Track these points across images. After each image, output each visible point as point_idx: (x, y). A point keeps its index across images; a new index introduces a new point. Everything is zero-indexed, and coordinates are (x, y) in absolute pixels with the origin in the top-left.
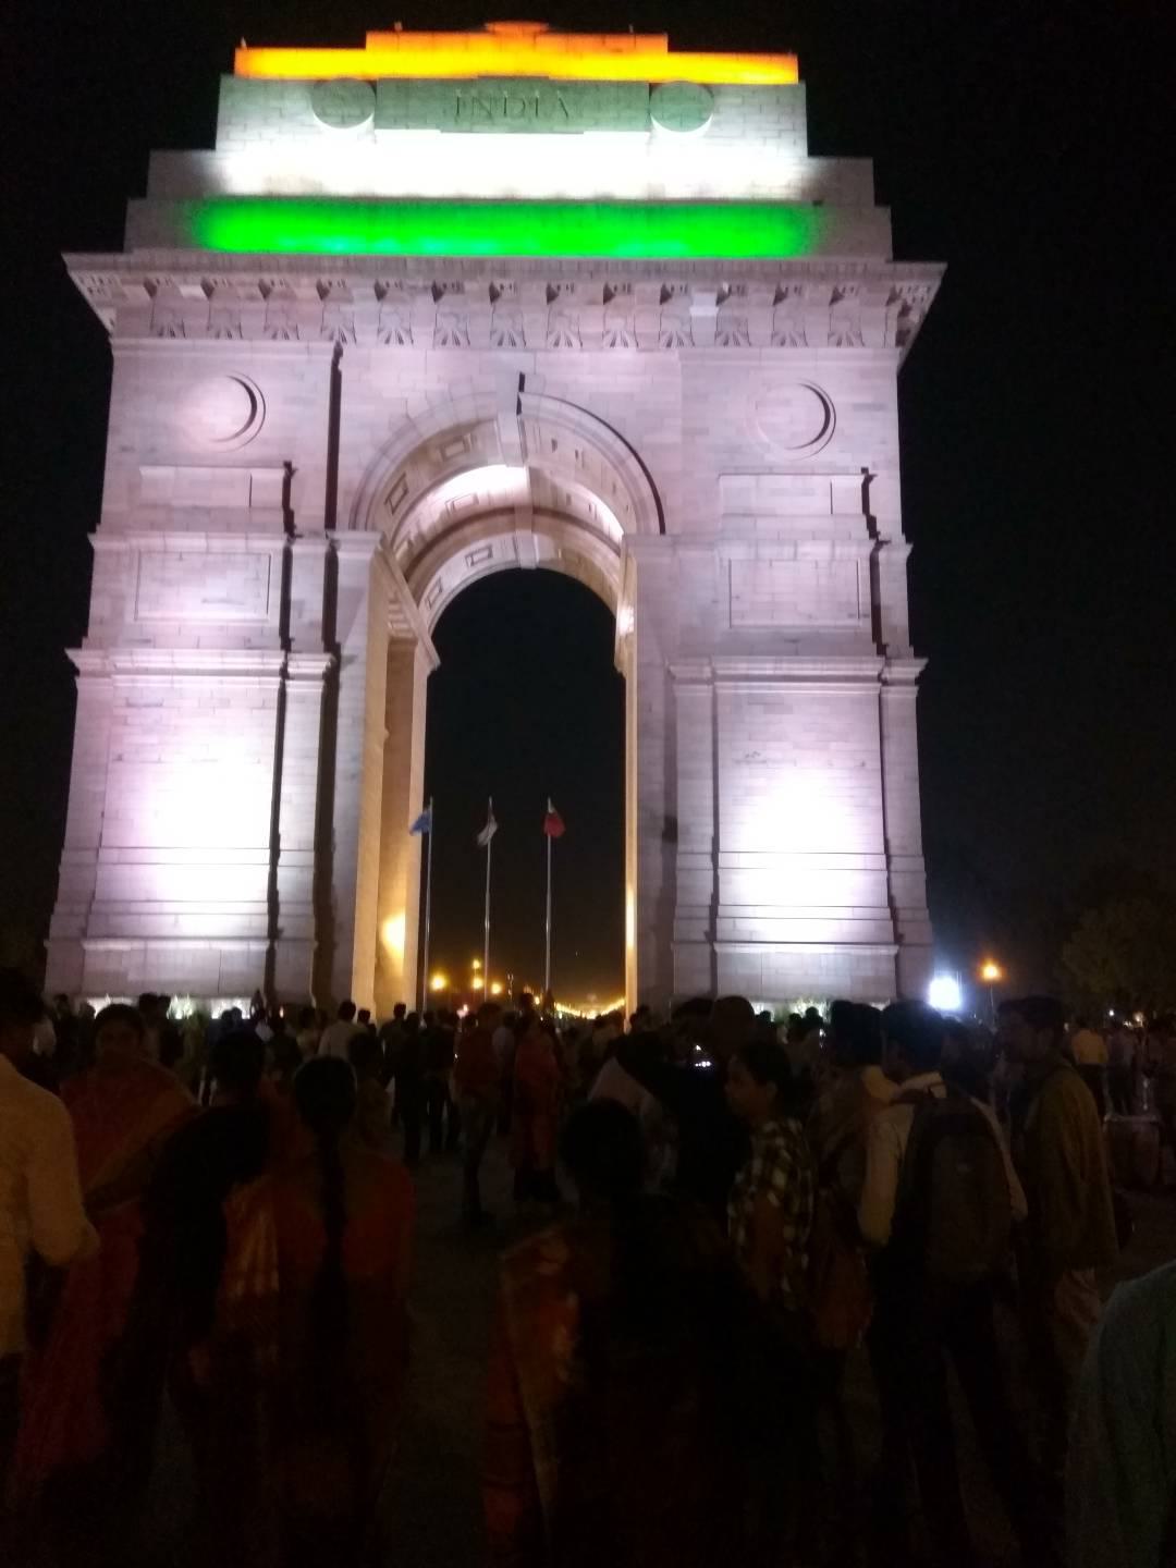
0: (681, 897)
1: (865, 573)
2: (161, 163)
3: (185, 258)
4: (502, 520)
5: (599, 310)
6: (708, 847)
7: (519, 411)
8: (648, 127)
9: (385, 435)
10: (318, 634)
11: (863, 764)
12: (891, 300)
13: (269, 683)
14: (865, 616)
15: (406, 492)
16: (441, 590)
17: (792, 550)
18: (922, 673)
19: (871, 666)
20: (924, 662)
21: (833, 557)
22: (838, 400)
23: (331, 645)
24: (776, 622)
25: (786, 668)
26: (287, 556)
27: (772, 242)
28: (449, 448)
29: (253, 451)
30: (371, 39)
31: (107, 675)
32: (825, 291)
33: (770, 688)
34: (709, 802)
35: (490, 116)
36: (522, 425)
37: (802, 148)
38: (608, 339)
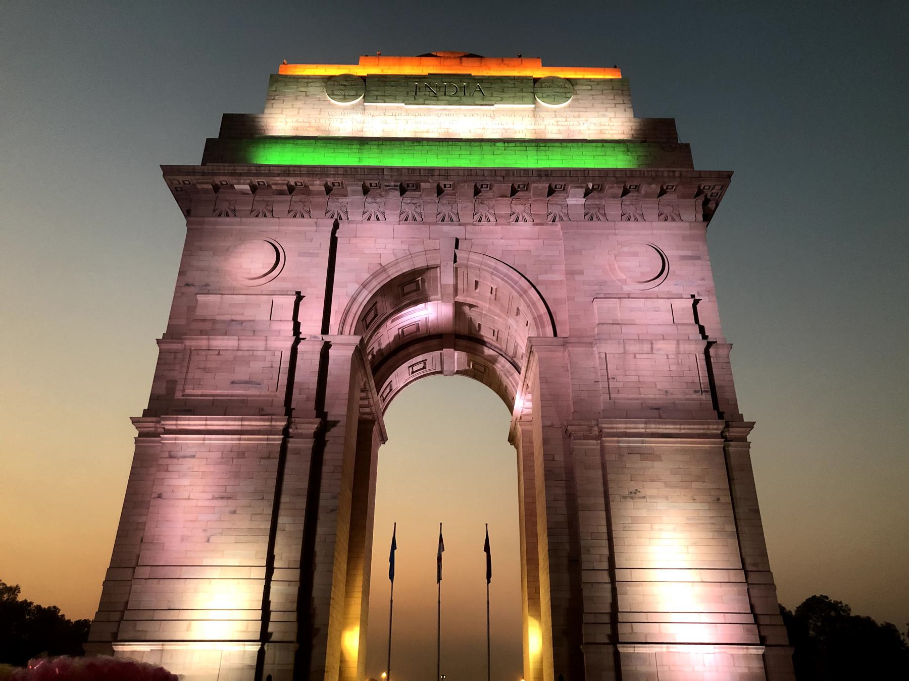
1: (702, 363)
3: (239, 169)
4: (434, 342)
5: (507, 201)
6: (605, 565)
7: (455, 261)
8: (534, 102)
9: (366, 276)
10: (312, 404)
11: (718, 499)
12: (698, 195)
15: (376, 315)
17: (649, 346)
21: (678, 353)
22: (667, 253)
25: (653, 428)
27: (618, 161)
28: (407, 287)
30: (362, 60)
31: (157, 435)
32: (655, 188)
34: (604, 529)
35: (435, 95)
36: (456, 270)
38: (514, 217)
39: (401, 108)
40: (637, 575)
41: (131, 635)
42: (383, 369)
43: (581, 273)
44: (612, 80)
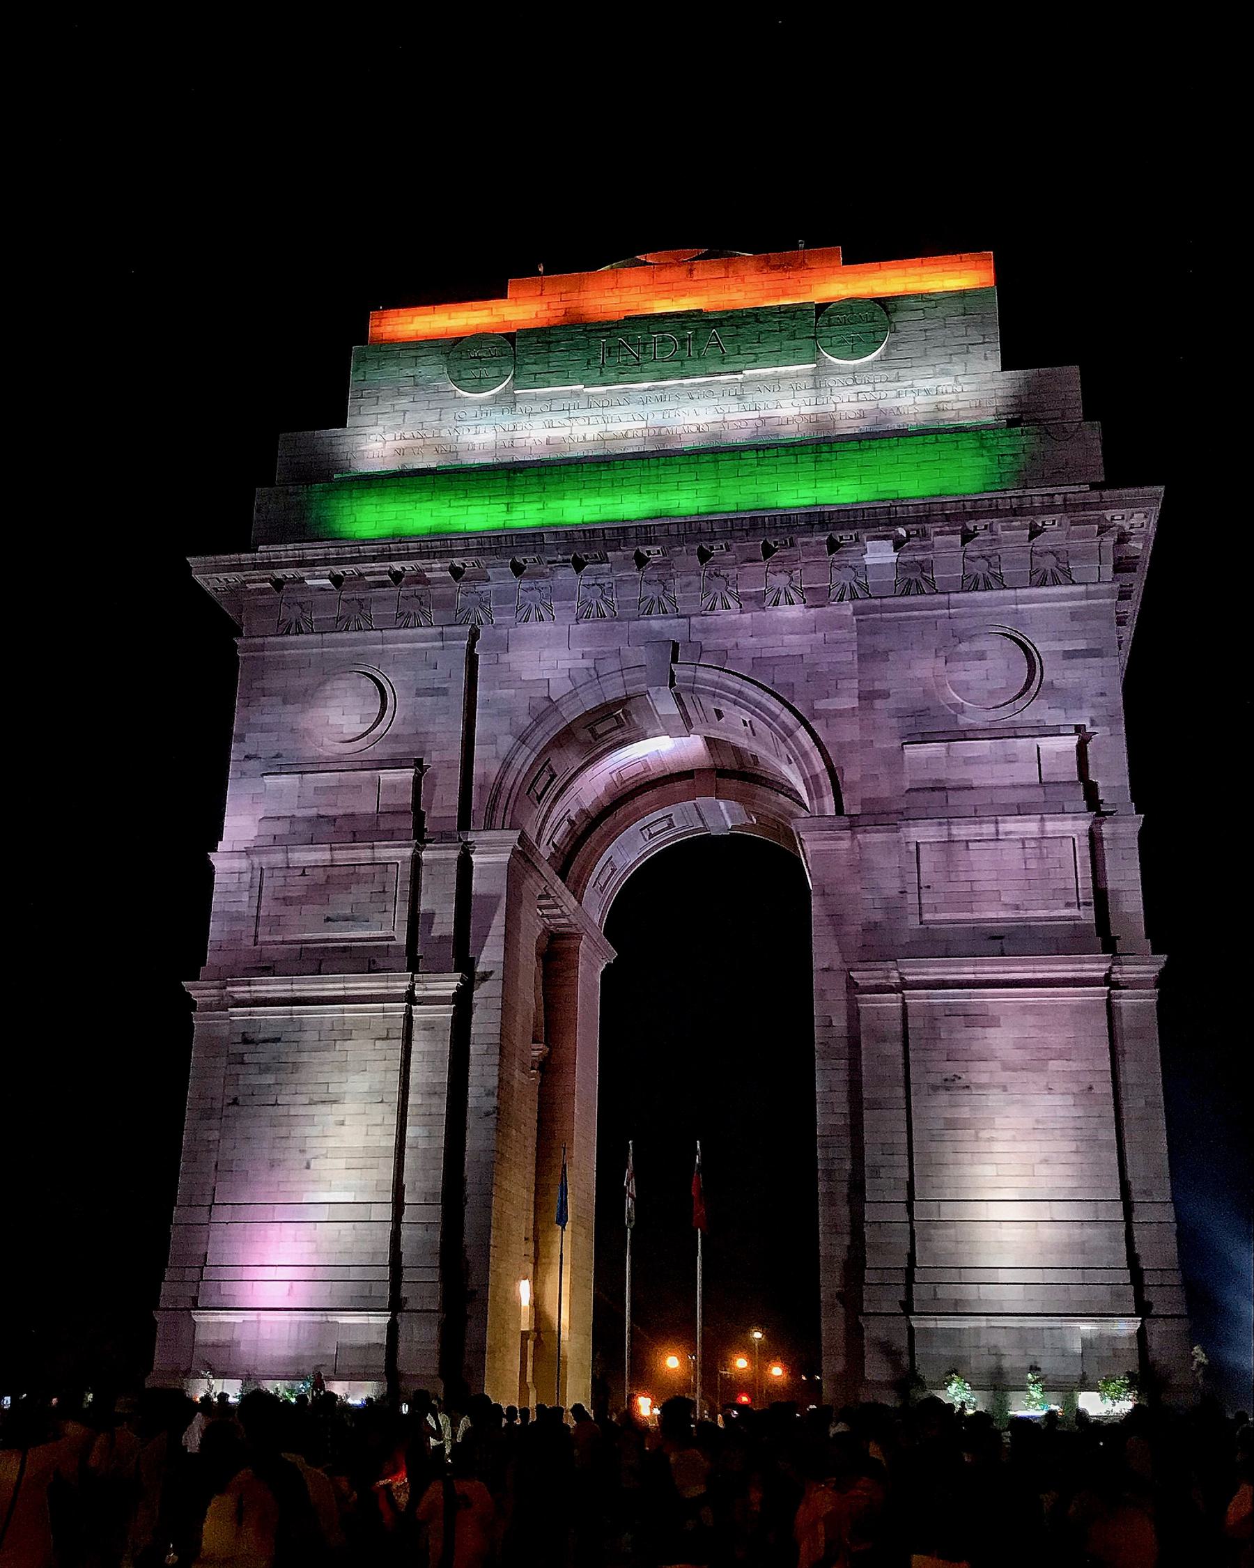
0: (871, 1260)
2: (290, 446)
5: (759, 568)
6: (903, 1196)
7: (672, 685)
11: (1091, 1088)
13: (392, 1010)
14: (1086, 904)
15: (553, 776)
16: (613, 870)
18: (1162, 972)
19: (1095, 966)
20: (1164, 958)
22: (1041, 646)
23: (465, 964)
24: (976, 915)
26: (416, 862)
29: (381, 751)
33: (970, 996)
36: (678, 698)
37: (998, 365)
39: (577, 394)
40: (948, 1211)
41: (215, 1301)
42: (574, 869)
43: (885, 695)
44: (962, 294)
